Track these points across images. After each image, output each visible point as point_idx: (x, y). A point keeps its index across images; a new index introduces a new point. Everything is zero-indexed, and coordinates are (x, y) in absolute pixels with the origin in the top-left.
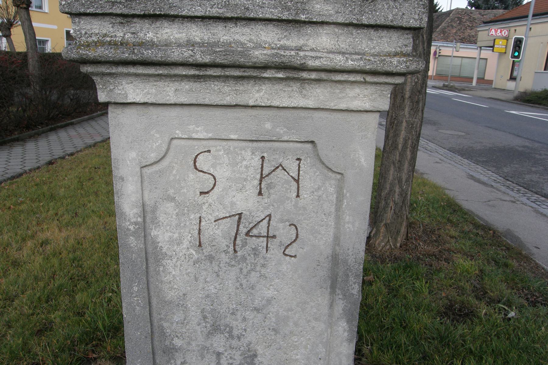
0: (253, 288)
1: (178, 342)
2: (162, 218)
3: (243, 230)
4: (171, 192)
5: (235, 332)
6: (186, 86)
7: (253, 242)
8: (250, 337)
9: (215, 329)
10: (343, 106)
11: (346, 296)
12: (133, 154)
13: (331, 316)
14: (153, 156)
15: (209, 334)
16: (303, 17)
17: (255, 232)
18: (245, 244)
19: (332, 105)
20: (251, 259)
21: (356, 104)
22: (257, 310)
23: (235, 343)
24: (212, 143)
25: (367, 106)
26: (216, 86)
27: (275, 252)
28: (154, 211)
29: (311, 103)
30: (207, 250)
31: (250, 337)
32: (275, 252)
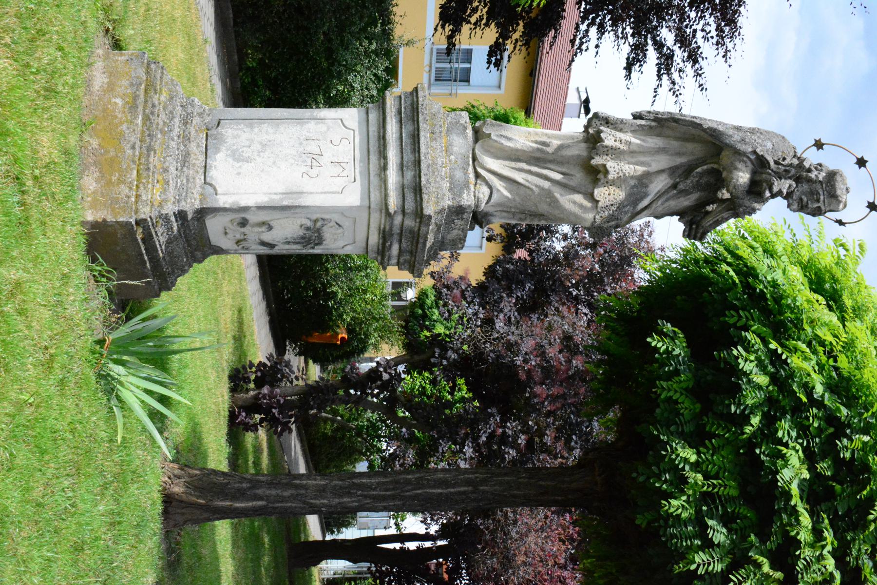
0: (286, 161)
1: (256, 130)
2: (320, 126)
3: (314, 156)
4: (331, 129)
5: (262, 154)
6: (376, 134)
7: (309, 160)
8: (259, 160)
9: (264, 146)
10: (371, 190)
11: (282, 200)
12: (347, 116)
13: (270, 194)
14: (346, 123)
15: (261, 143)
16: (405, 169)
17: (314, 161)
18: (308, 157)
19: (372, 186)
20: (301, 159)
21: (372, 195)
22: (274, 163)
23: (256, 153)
24: (276, 215)
25: (372, 199)
26: (377, 145)
27: (304, 169)
28: (324, 123)
29: (372, 178)
30: (305, 143)
31: (259, 160)
32: (304, 169)
